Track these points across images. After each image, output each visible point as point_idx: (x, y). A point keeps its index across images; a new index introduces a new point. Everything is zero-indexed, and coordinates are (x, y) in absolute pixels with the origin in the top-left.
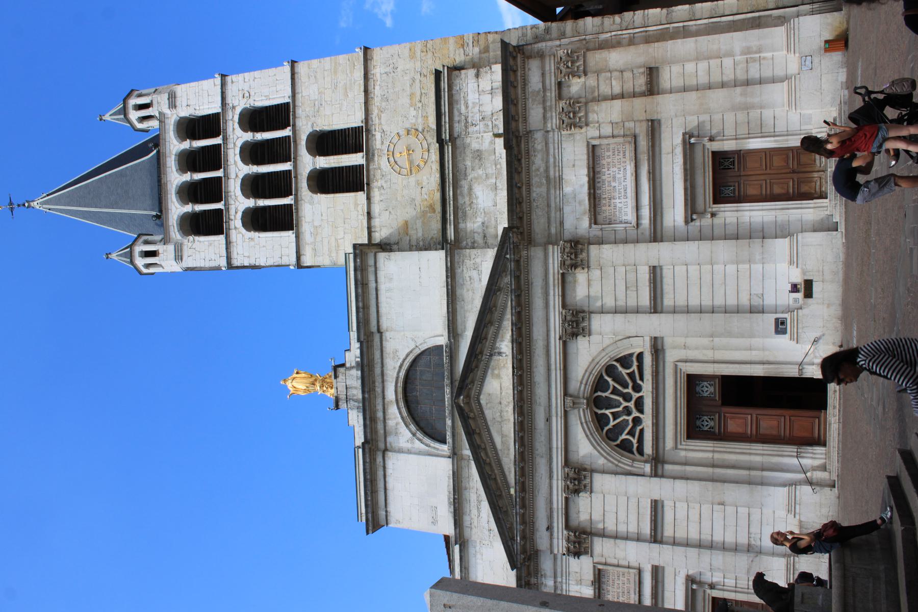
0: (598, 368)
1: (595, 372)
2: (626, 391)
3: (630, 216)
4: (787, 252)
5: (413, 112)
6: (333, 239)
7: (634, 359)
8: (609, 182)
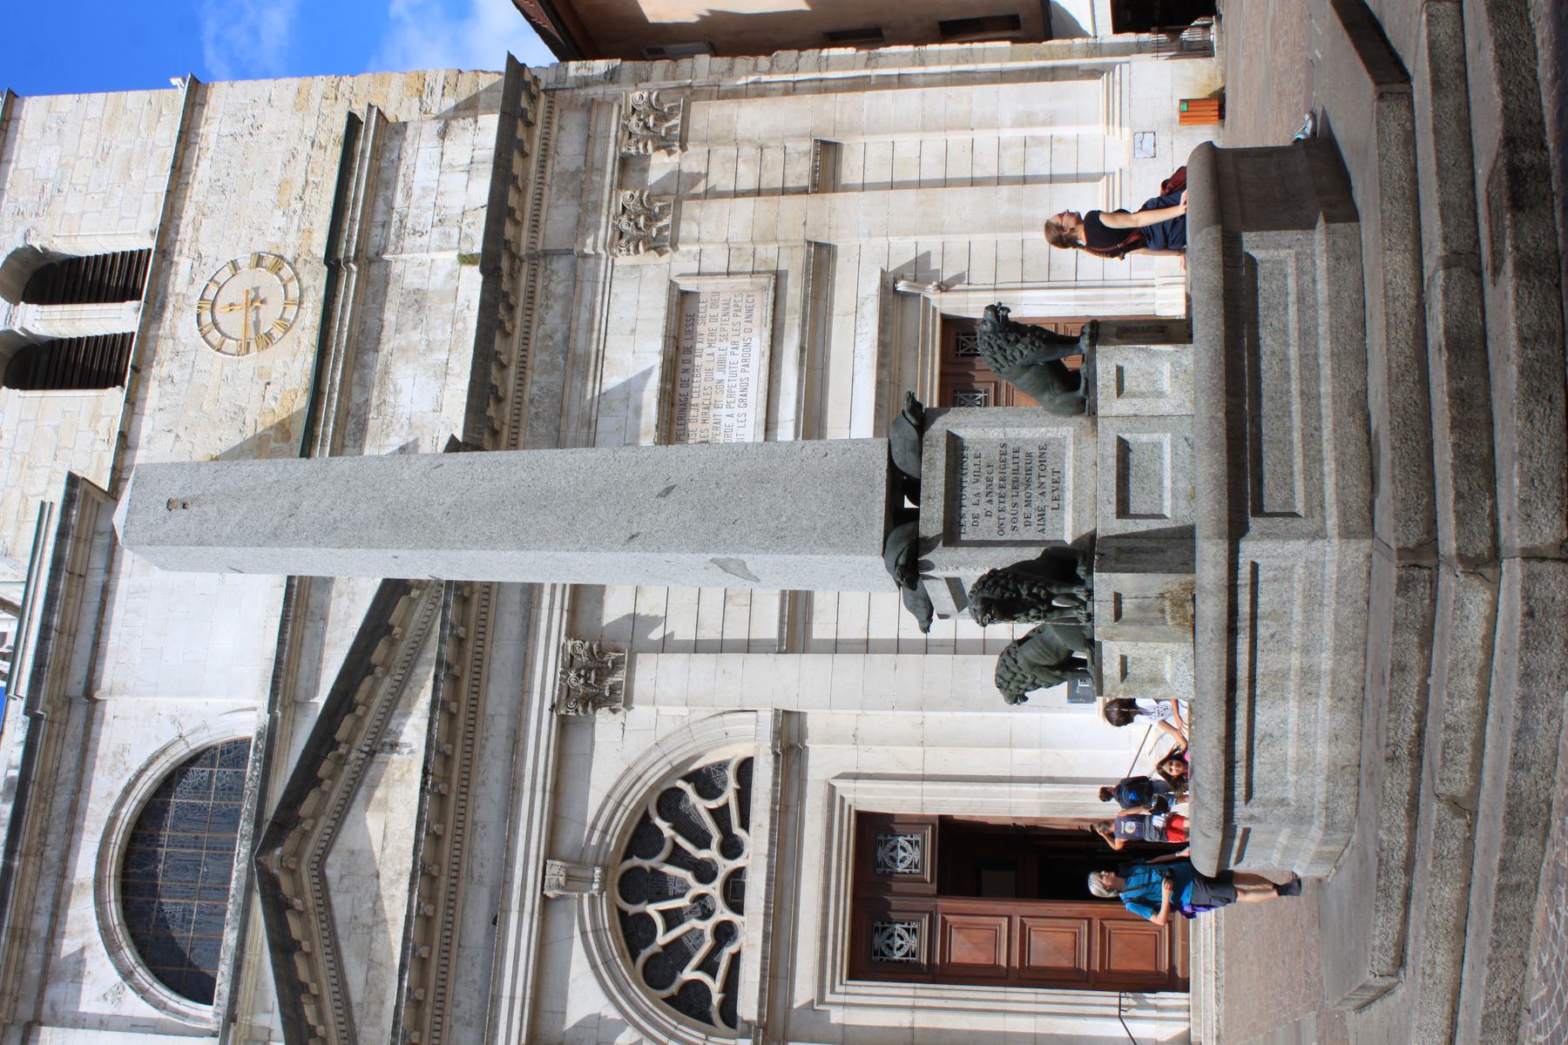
0: (640, 790)
1: (631, 802)
2: (702, 854)
3: (748, 430)
5: (279, 220)
6: (16, 494)
7: (731, 774)
8: (709, 370)
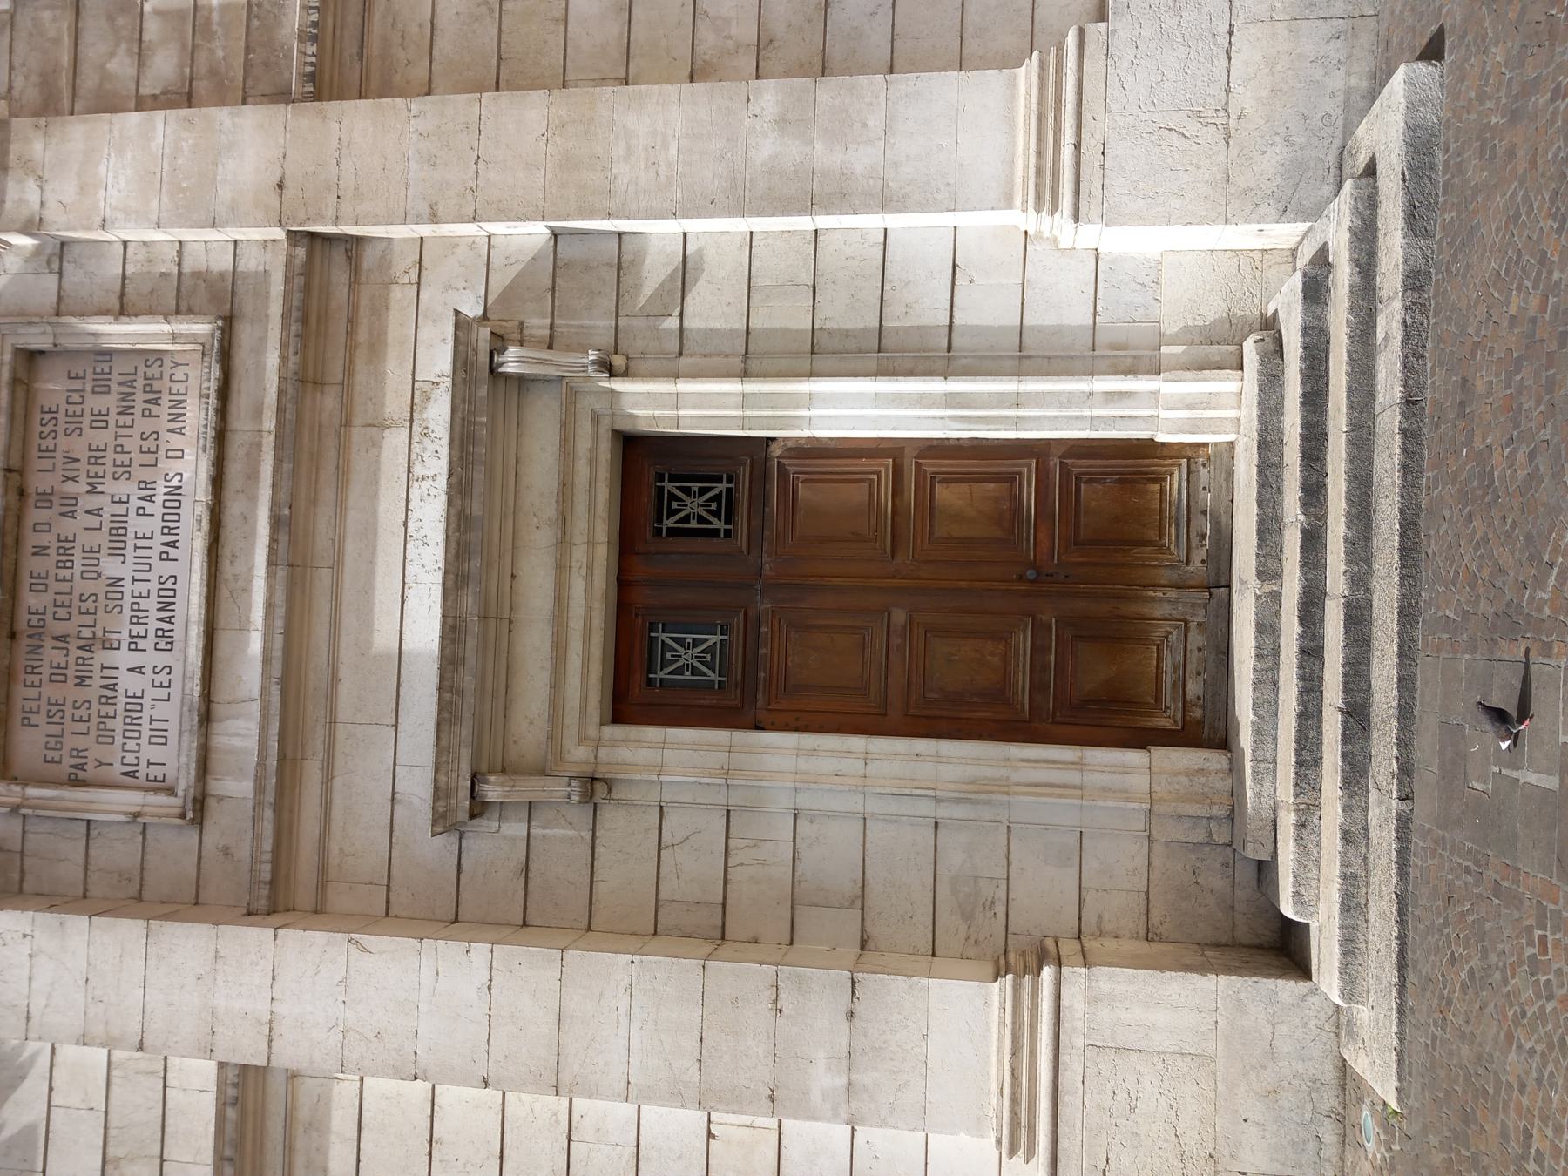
4: (996, 1070)
8: (91, 553)
